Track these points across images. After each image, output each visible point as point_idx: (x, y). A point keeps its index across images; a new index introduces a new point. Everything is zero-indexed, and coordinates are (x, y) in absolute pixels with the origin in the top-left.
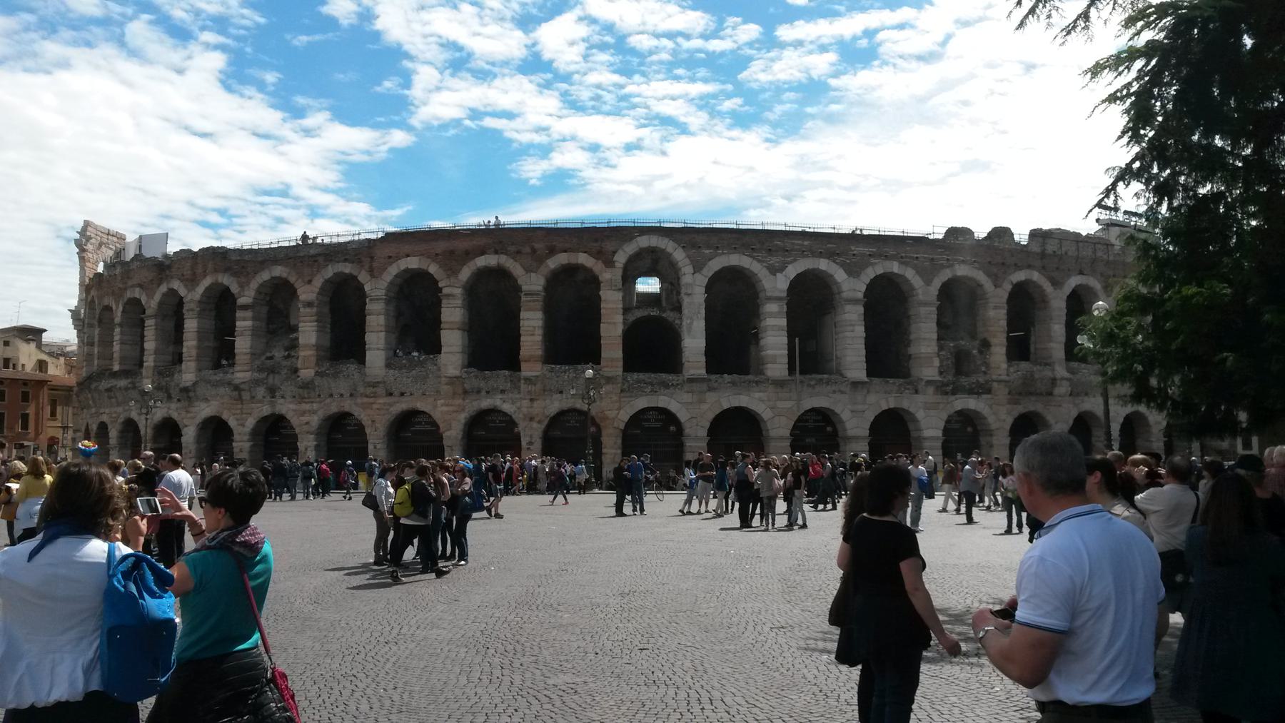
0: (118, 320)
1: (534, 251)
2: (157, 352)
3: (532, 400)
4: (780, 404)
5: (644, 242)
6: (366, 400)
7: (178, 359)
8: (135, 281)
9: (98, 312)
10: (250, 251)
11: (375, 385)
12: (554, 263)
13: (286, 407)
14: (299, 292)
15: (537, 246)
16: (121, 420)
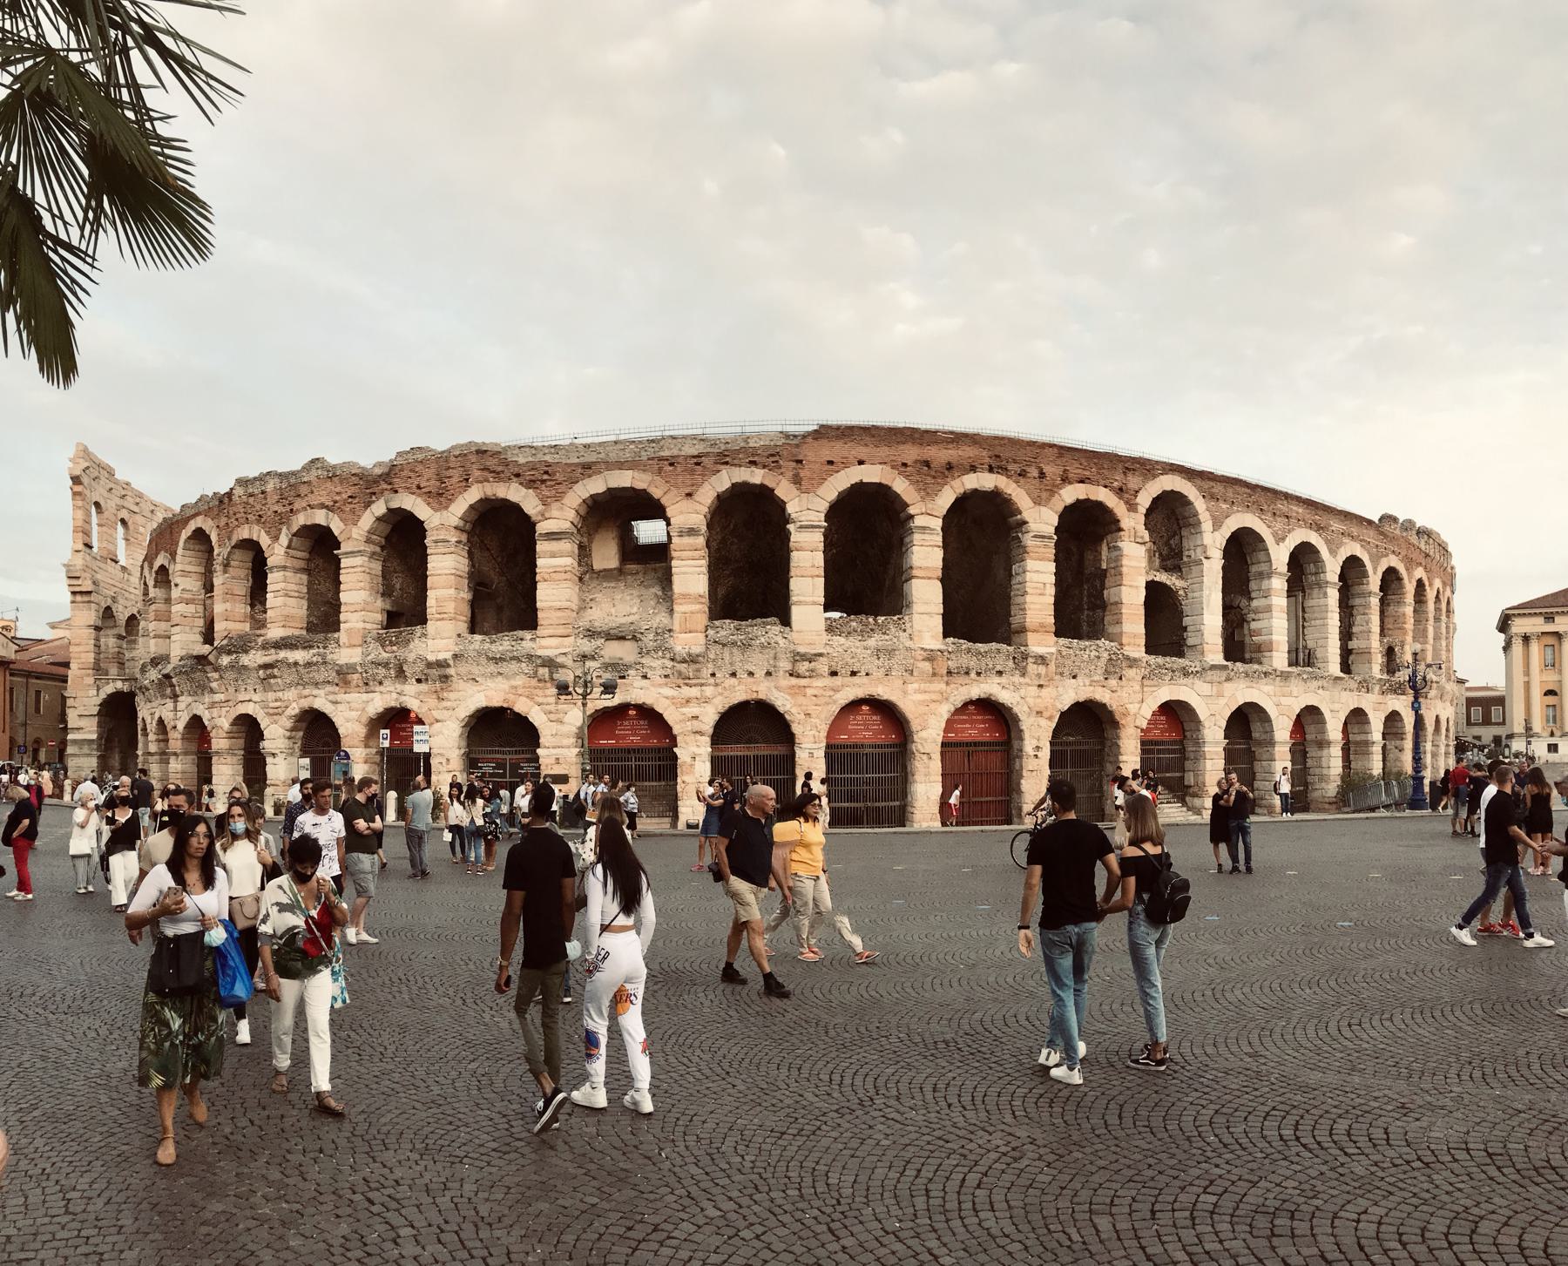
4: (1285, 701)
6: (794, 681)
11: (811, 658)
16: (294, 709)
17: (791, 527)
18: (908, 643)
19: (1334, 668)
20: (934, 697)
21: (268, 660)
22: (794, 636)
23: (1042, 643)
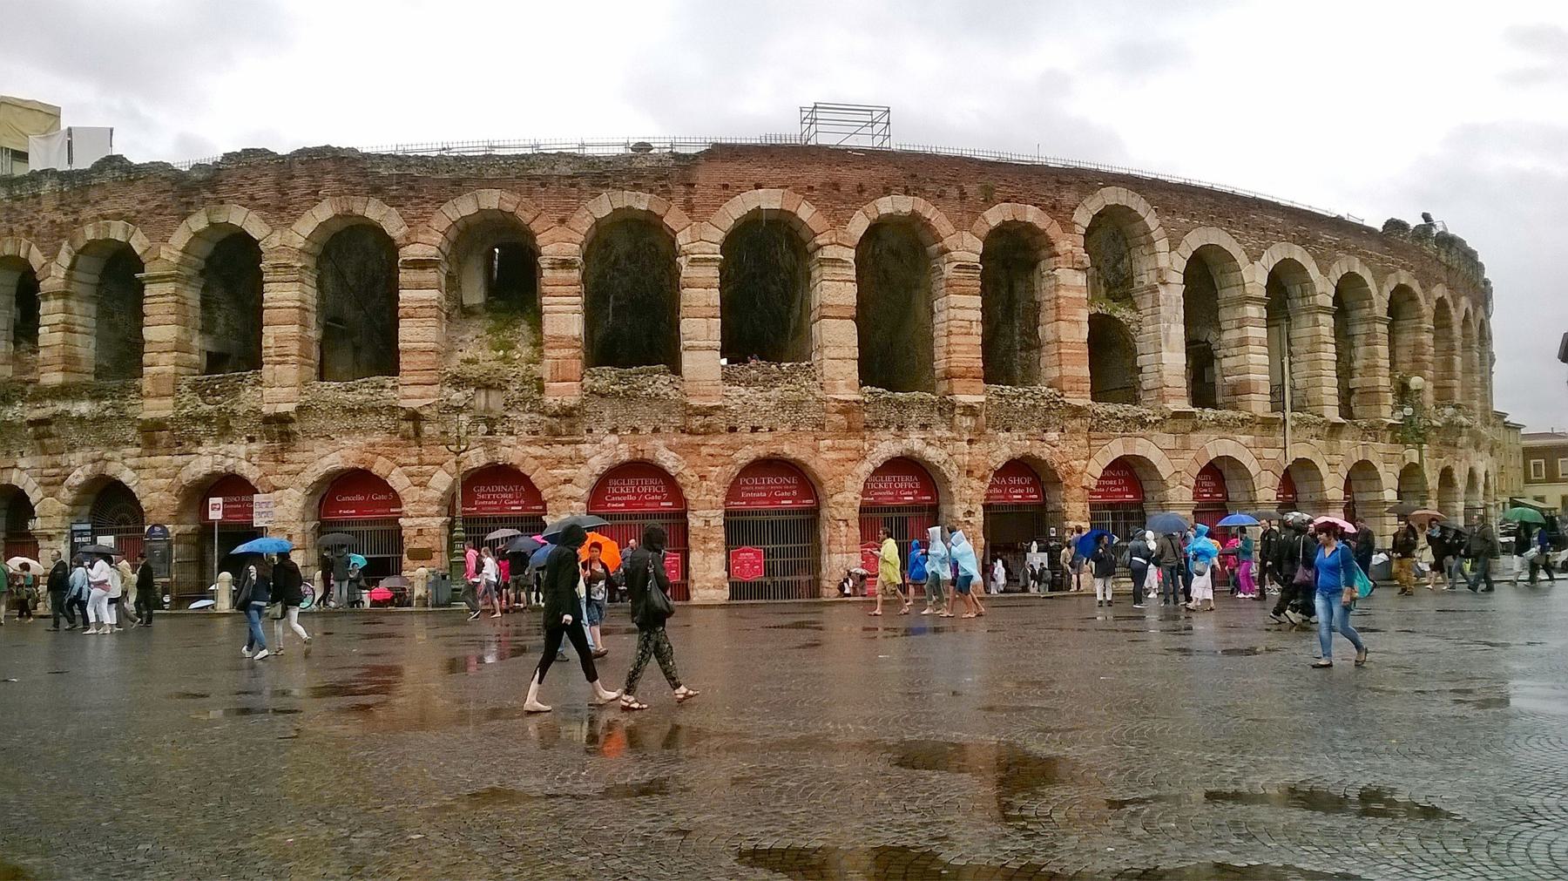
0: (45, 286)
1: (963, 196)
2: (181, 347)
4: (1270, 454)
6: (686, 438)
7: (251, 358)
8: (109, 207)
10: (423, 161)
12: (995, 216)
14: (540, 240)
15: (972, 189)
16: (78, 477)
17: (682, 261)
18: (818, 393)
19: (1333, 414)
20: (850, 455)
21: (38, 414)
22: (688, 386)
23: (971, 395)
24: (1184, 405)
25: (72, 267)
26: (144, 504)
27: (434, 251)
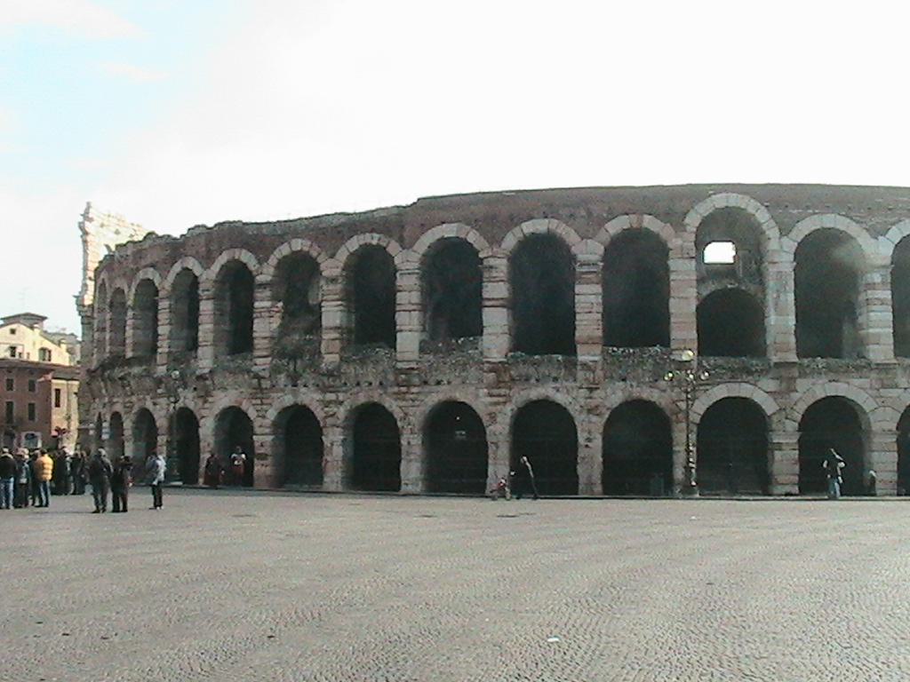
0: (130, 303)
3: (591, 390)
5: (720, 201)
7: (193, 345)
9: (109, 295)
12: (615, 227)
13: (310, 397)
14: (322, 267)
24: (793, 358)
25: (135, 295)
26: (158, 424)
27: (269, 278)
